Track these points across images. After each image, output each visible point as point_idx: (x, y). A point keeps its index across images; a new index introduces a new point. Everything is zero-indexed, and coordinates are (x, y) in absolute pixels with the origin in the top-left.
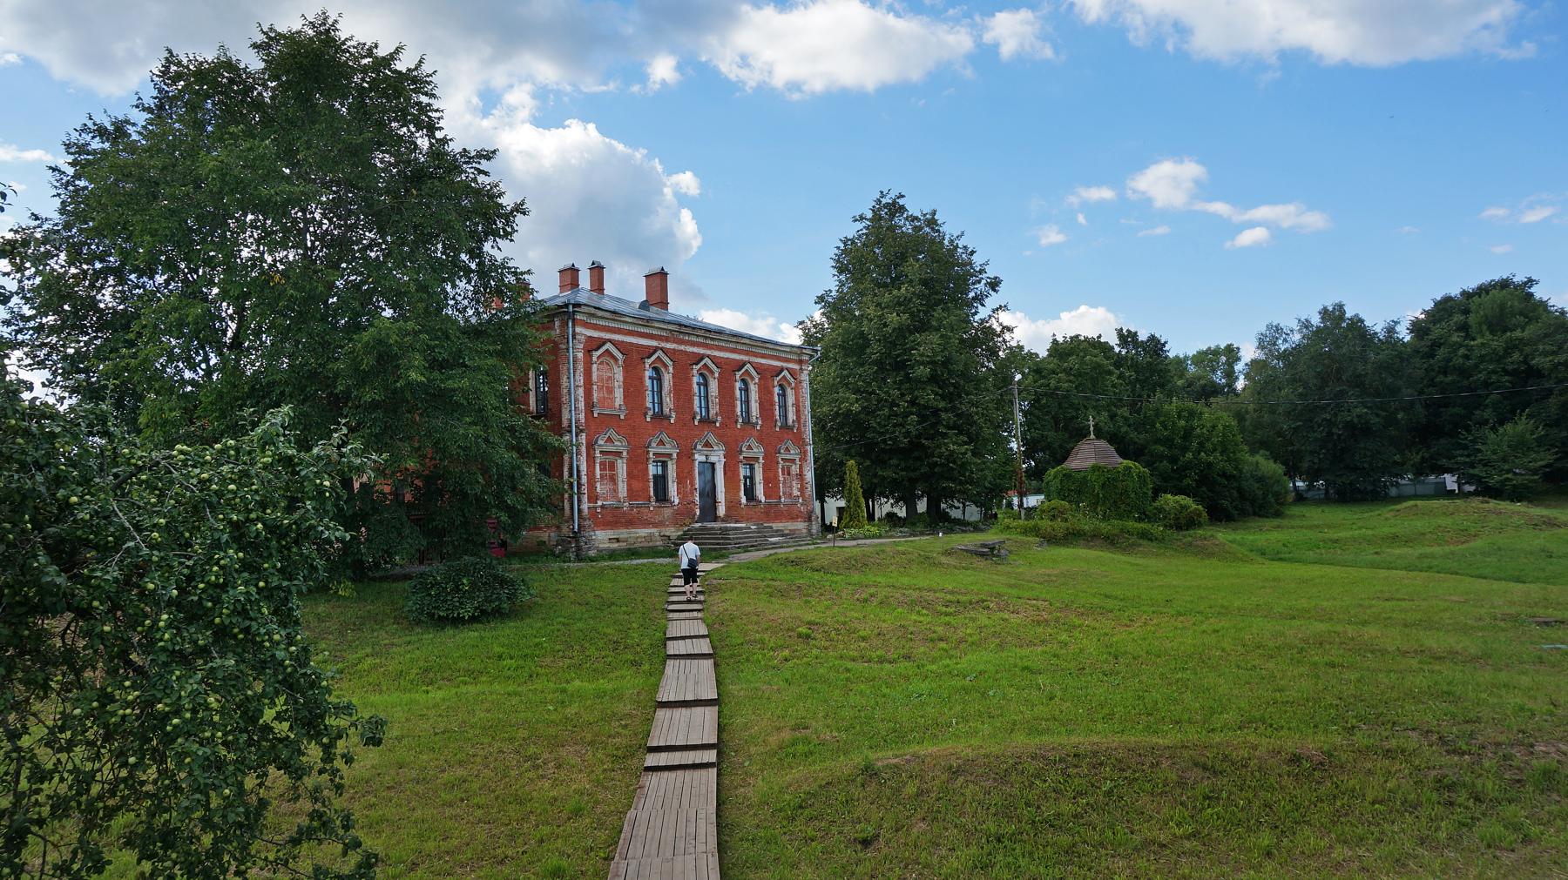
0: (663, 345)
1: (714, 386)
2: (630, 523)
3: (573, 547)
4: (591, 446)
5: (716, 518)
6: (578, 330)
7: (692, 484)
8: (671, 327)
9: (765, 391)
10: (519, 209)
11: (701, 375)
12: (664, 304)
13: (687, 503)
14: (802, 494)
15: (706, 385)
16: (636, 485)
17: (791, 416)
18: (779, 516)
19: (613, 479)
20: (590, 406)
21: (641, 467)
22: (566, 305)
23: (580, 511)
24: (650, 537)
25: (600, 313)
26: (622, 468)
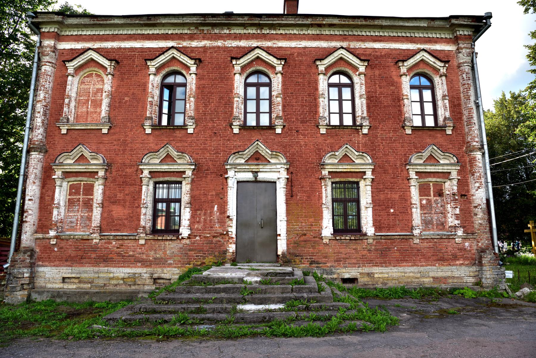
2: (105, 259)
7: (223, 209)
16: (118, 211)
19: (88, 205)
24: (134, 279)
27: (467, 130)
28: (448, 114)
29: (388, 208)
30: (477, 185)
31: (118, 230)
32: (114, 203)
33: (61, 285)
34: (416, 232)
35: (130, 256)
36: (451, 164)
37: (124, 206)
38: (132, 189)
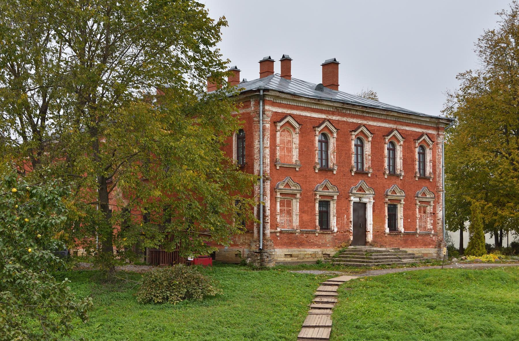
0: (330, 117)
1: (368, 148)
2: (300, 244)
3: (258, 261)
4: (273, 190)
5: (365, 243)
6: (267, 107)
7: (348, 218)
8: (336, 105)
9: (408, 151)
10: (222, 23)
11: (359, 138)
12: (335, 86)
13: (344, 232)
14: (435, 228)
15: (362, 146)
16: (306, 217)
17: (429, 169)
18: (414, 243)
19: (289, 213)
20: (274, 162)
21: (310, 205)
22: (258, 90)
23: (264, 234)
24: (314, 255)
25: (283, 96)
26: (296, 206)
27: (437, 180)
28: (431, 171)
29: (408, 219)
30: (440, 209)
31: (306, 228)
32: (303, 212)
33: (284, 259)
34: (418, 231)
35: (312, 242)
36: (431, 198)
37: (308, 214)
38: (311, 205)
